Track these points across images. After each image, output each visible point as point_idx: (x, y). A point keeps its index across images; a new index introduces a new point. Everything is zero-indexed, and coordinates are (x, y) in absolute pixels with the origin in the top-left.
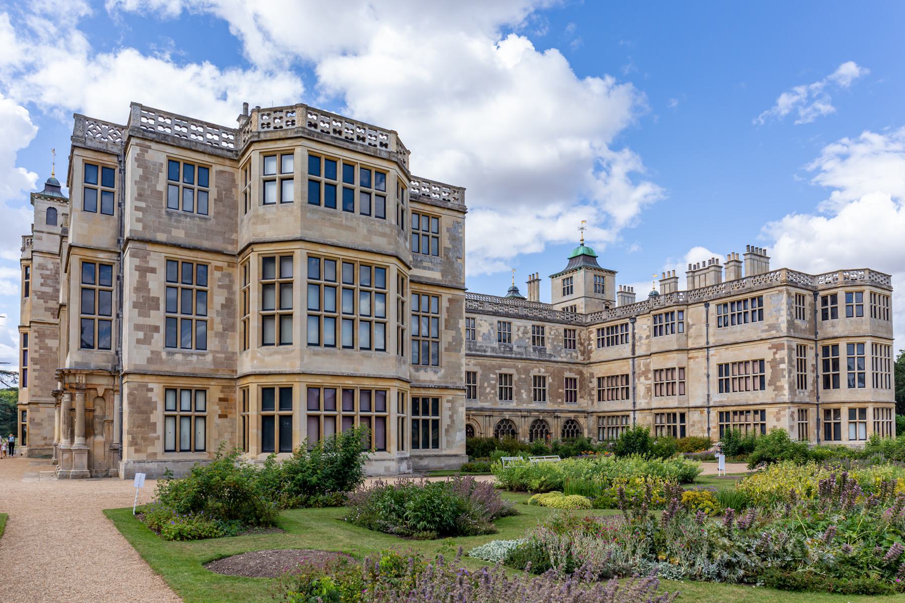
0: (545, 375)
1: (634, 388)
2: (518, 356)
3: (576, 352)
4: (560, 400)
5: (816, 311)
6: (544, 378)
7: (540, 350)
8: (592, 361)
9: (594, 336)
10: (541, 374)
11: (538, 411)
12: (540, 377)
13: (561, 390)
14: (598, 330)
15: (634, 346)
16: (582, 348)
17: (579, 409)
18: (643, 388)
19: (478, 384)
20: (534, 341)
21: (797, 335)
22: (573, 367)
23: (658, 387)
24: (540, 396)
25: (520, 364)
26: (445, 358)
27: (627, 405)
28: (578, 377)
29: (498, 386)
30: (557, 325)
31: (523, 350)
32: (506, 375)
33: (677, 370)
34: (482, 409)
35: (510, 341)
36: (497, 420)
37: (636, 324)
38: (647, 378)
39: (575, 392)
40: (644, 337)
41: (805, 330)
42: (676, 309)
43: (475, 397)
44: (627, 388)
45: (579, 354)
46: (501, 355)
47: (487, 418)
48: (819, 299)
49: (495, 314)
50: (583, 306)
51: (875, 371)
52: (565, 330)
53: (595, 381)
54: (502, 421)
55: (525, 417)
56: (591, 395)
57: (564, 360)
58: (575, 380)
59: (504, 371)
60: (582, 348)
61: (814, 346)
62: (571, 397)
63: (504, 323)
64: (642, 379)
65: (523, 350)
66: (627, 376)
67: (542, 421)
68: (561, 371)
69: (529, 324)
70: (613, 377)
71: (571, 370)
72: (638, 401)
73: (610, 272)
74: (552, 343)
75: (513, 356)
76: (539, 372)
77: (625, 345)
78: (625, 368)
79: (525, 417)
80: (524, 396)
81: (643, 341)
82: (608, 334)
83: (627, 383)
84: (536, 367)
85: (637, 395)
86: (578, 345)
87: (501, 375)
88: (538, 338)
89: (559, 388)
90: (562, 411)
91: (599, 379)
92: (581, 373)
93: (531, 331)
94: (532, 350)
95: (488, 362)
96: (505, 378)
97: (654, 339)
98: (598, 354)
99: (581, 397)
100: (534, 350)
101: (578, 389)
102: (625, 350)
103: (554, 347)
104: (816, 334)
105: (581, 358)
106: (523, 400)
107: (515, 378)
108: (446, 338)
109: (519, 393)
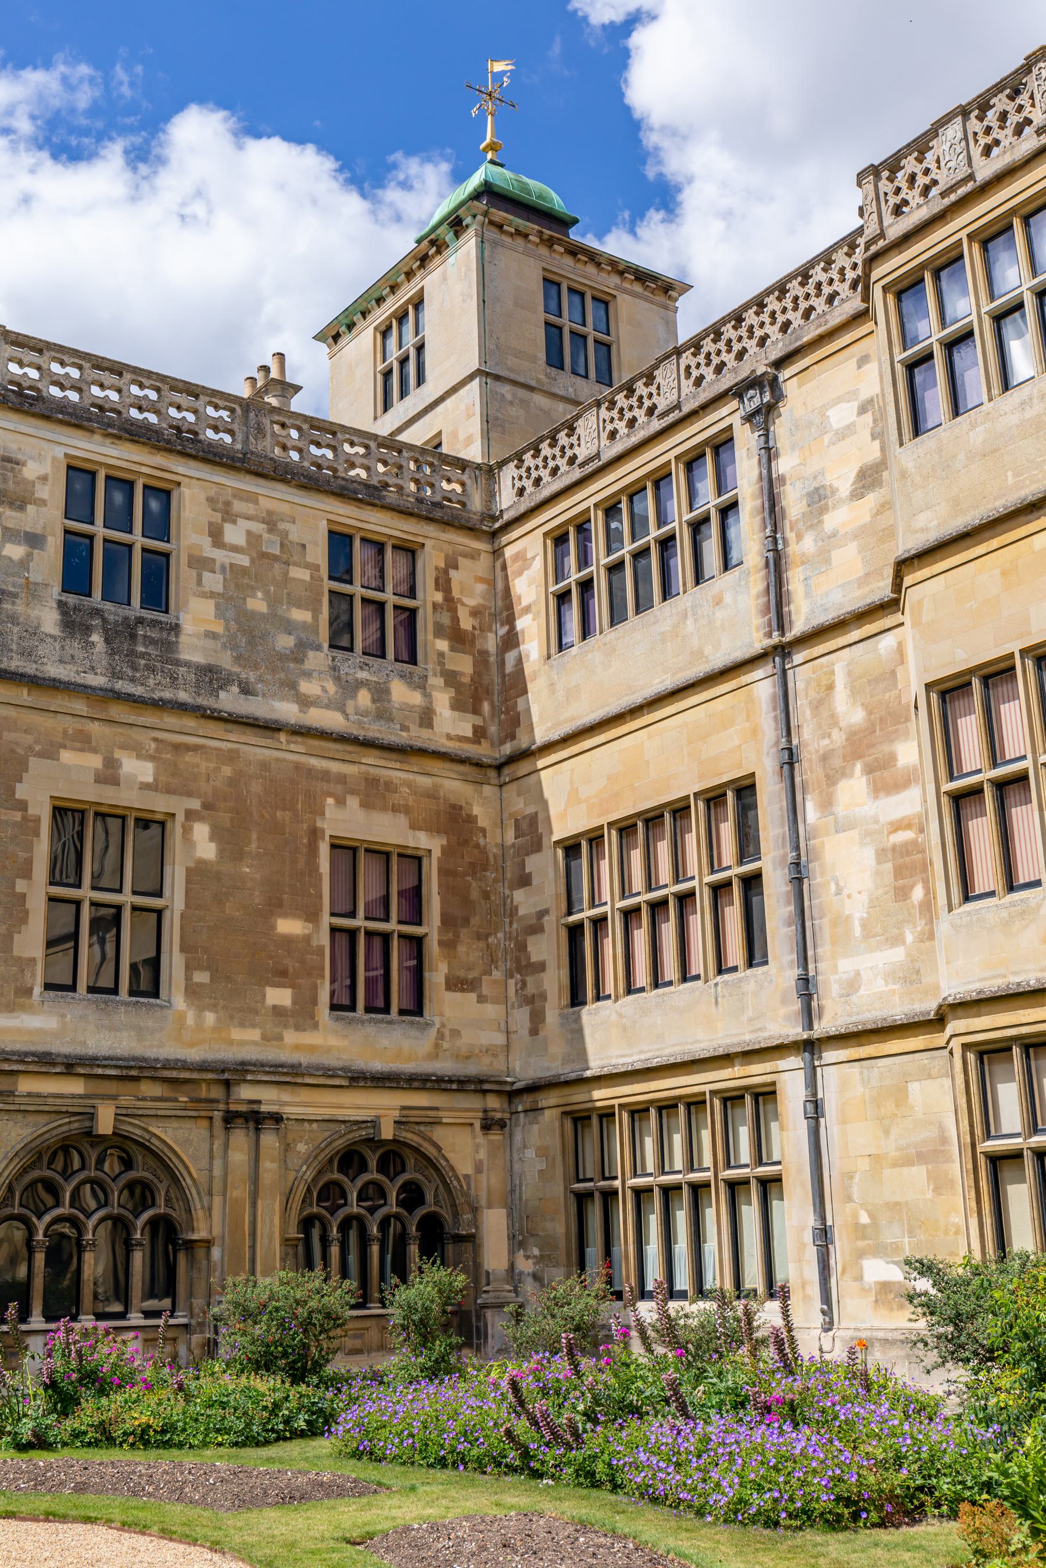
0: (160, 804)
1: (798, 876)
3: (421, 685)
4: (279, 996)
7: (122, 635)
9: (530, 585)
11: (70, 1066)
13: (289, 926)
14: (560, 540)
15: (776, 564)
16: (464, 665)
17: (444, 1066)
18: (869, 855)
20: (75, 576)
22: (393, 771)
23: (982, 830)
27: (750, 1007)
30: (276, 497)
37: (781, 428)
38: (885, 779)
39: (417, 944)
40: (845, 486)
44: (752, 883)
45: (442, 700)
50: (474, 426)
52: (340, 542)
53: (547, 866)
56: (526, 967)
57: (331, 720)
60: (464, 665)
62: (379, 975)
64: (853, 790)
66: (745, 790)
67: (125, 1147)
68: (301, 792)
70: (652, 819)
71: (374, 794)
72: (834, 970)
73: (643, 276)
74: (228, 603)
76: (109, 775)
77: (722, 584)
78: (730, 737)
81: (836, 519)
82: (612, 540)
83: (748, 843)
84: (84, 742)
85: (822, 926)
86: (434, 645)
88: (118, 555)
89: (275, 906)
91: (571, 848)
92: (455, 822)
97: (912, 456)
98: (559, 690)
99: (455, 984)
102: (722, 615)
103: (247, 633)
105: (451, 725)
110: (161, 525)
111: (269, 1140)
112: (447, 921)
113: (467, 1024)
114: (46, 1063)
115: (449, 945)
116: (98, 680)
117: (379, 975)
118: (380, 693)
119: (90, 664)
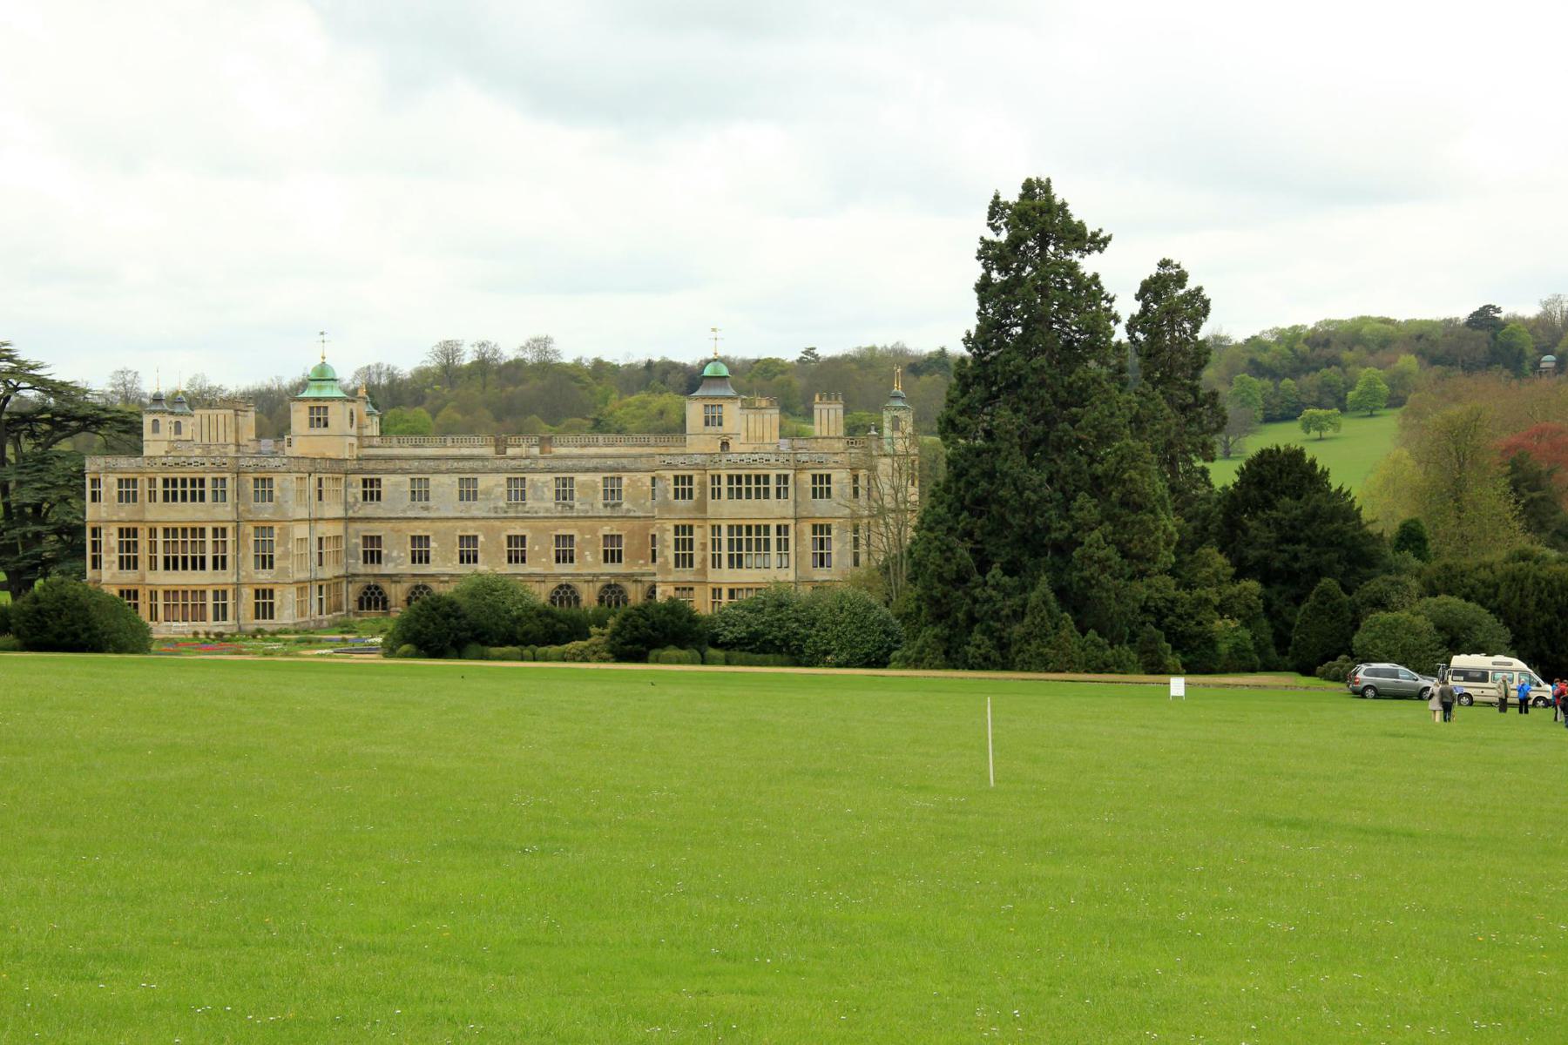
19: (527, 548)
24: (612, 556)
25: (581, 523)
26: (276, 565)
29: (553, 548)
30: (639, 475)
31: (587, 507)
34: (529, 575)
36: (552, 585)
41: (689, 511)
49: (550, 470)
54: (561, 587)
59: (561, 532)
65: (587, 507)
69: (598, 478)
80: (589, 558)
87: (558, 537)
90: (643, 575)
93: (601, 485)
95: (540, 524)
100: (606, 506)
106: (589, 565)
107: (576, 539)
108: (277, 553)
109: (582, 556)
110: (620, 485)
119: (608, 512)
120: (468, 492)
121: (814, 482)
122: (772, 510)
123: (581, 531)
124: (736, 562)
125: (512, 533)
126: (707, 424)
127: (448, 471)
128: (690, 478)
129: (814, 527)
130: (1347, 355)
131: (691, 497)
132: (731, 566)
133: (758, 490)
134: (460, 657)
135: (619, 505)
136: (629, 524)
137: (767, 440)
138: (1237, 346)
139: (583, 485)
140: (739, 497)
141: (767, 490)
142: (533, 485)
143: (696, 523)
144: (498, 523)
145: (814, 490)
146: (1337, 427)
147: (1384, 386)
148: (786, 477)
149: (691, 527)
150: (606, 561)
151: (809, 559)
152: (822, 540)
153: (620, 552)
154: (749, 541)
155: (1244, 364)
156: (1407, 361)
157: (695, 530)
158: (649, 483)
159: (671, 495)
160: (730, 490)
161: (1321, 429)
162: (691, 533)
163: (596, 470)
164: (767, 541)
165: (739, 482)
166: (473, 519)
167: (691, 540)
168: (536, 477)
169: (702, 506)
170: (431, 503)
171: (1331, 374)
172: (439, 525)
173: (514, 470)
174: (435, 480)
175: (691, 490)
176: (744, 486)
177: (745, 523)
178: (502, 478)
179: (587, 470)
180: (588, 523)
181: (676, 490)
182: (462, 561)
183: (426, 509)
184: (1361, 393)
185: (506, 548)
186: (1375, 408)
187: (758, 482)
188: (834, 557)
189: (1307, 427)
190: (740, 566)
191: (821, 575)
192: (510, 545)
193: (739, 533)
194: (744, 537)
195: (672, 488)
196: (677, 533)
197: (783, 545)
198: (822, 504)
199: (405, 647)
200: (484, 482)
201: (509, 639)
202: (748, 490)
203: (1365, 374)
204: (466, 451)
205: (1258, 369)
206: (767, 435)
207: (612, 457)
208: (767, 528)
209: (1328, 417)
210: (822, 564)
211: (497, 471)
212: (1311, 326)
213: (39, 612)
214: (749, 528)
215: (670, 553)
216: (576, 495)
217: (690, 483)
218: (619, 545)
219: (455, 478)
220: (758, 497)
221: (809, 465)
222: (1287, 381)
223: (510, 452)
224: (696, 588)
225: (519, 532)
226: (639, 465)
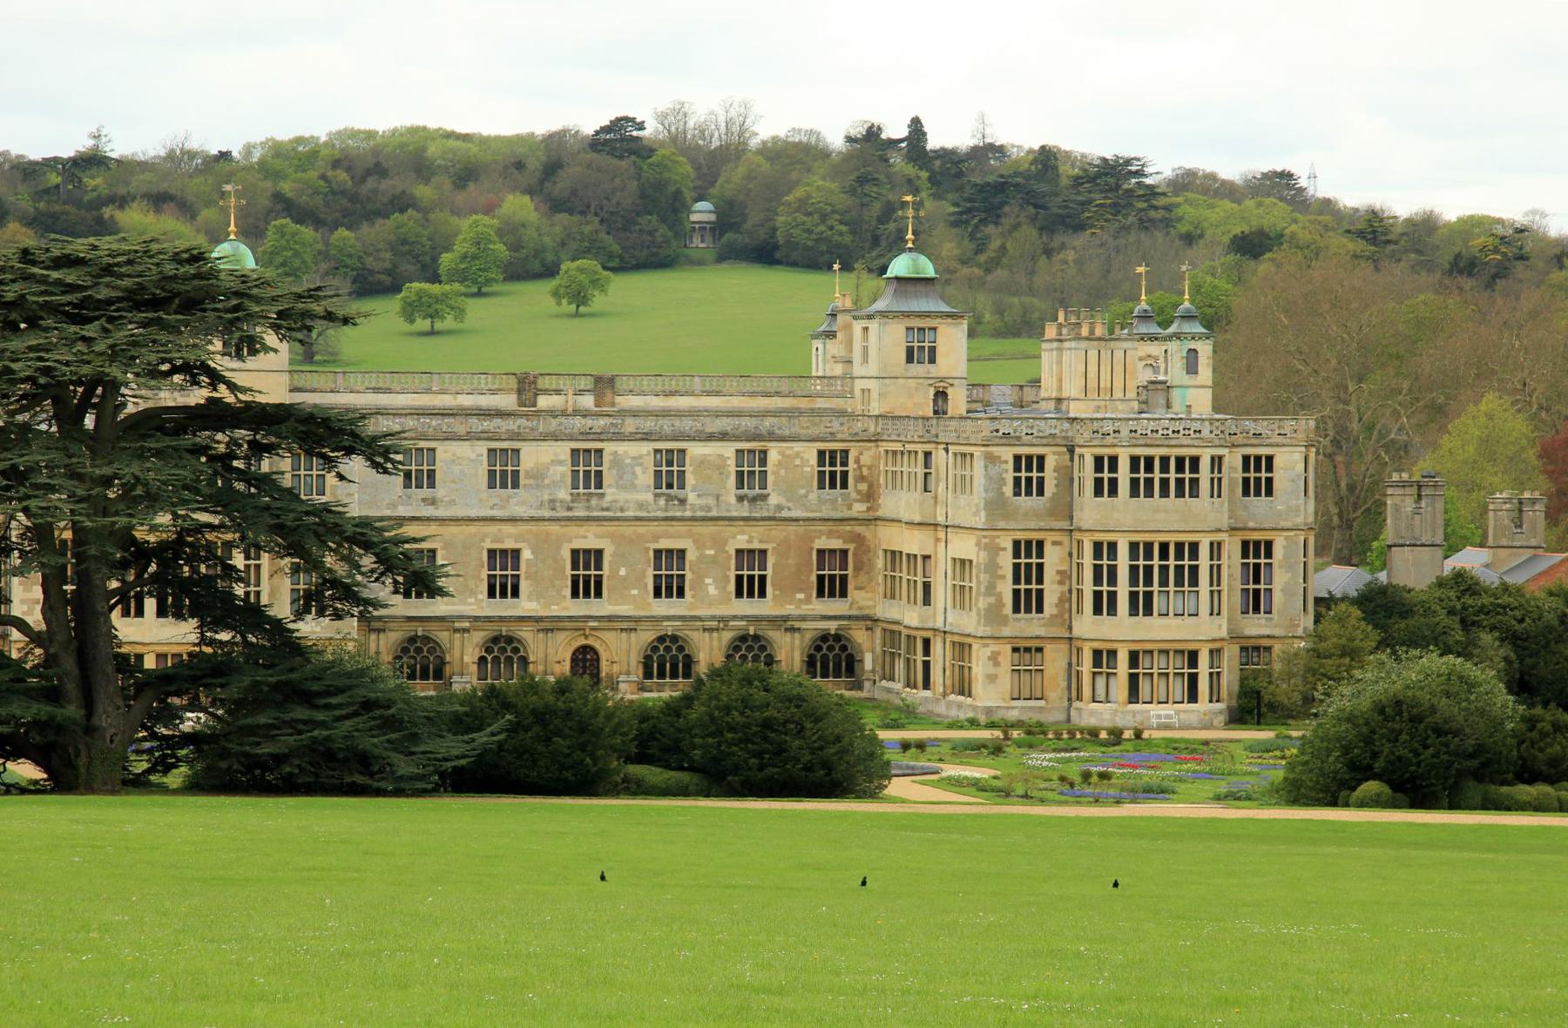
2: (699, 514)
4: (801, 596)
5: (1072, 480)
6: (763, 552)
8: (880, 513)
10: (756, 545)
12: (751, 552)
17: (854, 612)
19: (606, 572)
21: (1012, 525)
24: (750, 586)
28: (851, 547)
29: (651, 572)
31: (711, 501)
32: (670, 552)
33: (919, 560)
34: (610, 618)
35: (682, 486)
36: (647, 636)
42: (921, 448)
43: (599, 594)
46: (659, 514)
47: (624, 634)
48: (1076, 458)
49: (646, 437)
51: (1141, 588)
53: (881, 553)
54: (661, 639)
55: (711, 630)
58: (845, 552)
59: (664, 544)
61: (1065, 539)
63: (669, 452)
65: (711, 501)
67: (756, 638)
69: (728, 450)
71: (830, 534)
75: (688, 514)
79: (711, 630)
80: (712, 590)
84: (743, 533)
87: (658, 553)
90: (803, 618)
92: (859, 539)
93: (732, 463)
94: (733, 500)
95: (627, 530)
96: (671, 558)
99: (857, 588)
100: (740, 499)
101: (850, 572)
104: (1071, 518)
105: (859, 508)
106: (711, 597)
107: (690, 556)
109: (699, 583)
110: (763, 462)
111: (797, 635)
112: (857, 569)
113: (862, 598)
114: (735, 618)
115: (856, 577)
116: (746, 514)
117: (832, 586)
118: (833, 501)
119: (744, 510)
120: (504, 475)
121: (1246, 468)
122: (1196, 517)
123: (699, 543)
124: (1142, 605)
125: (580, 544)
126: (910, 359)
127: (470, 437)
128: (1041, 459)
129: (1245, 544)
130: (423, 192)
131: (1041, 492)
132: (1134, 611)
133: (1180, 482)
134: (1454, 806)
135: (764, 497)
136: (779, 532)
137: (1118, 394)
138: (1448, 224)
139: (702, 462)
140: (1149, 493)
141: (1195, 483)
142: (617, 461)
143: (1049, 538)
144: (555, 528)
145: (1246, 481)
146: (460, 313)
147: (500, 247)
148: (1220, 458)
149: (1040, 544)
150: (739, 594)
151: (1238, 598)
152: (1257, 567)
153: (763, 579)
154: (1164, 570)
155: (264, 201)
156: (519, 206)
157: (1048, 548)
158: (814, 460)
159: (1009, 489)
160: (1134, 483)
161: (433, 316)
162: (1040, 555)
163: (723, 437)
164: (1194, 570)
165: (1149, 468)
166: (513, 520)
167: (1040, 567)
168: (623, 448)
169: (1065, 509)
170: (440, 492)
171: (406, 221)
172: (453, 530)
173: (586, 435)
174: (444, 451)
175: (1041, 481)
176: (1157, 475)
177: (1158, 539)
178: (563, 450)
179: (710, 438)
180: (707, 530)
181: (1017, 481)
182: (491, 594)
183: (432, 502)
184: (464, 257)
185: (569, 572)
186: (489, 281)
187: (1180, 467)
188: (1277, 597)
189: (409, 313)
190: (1148, 611)
191: (1256, 626)
192: (575, 566)
193: (1149, 556)
194: (1156, 562)
195: (1010, 476)
196: (1017, 555)
197: (1216, 573)
198: (1259, 504)
199: (1372, 787)
200: (533, 456)
201: (1529, 776)
202: (1165, 483)
203: (468, 228)
204: (466, 401)
205: (285, 206)
206: (1118, 385)
207: (751, 414)
208: (1194, 547)
209: (445, 295)
210: (1257, 609)
211: (556, 437)
212: (323, 139)
213: (767, 725)
214: (1164, 547)
215: (1006, 588)
216: (690, 479)
217: (1041, 468)
218: (763, 567)
219: (482, 448)
220: (1180, 493)
221: (1239, 439)
222: (342, 232)
223: (544, 402)
224: (1049, 648)
225: (591, 543)
226: (796, 430)
